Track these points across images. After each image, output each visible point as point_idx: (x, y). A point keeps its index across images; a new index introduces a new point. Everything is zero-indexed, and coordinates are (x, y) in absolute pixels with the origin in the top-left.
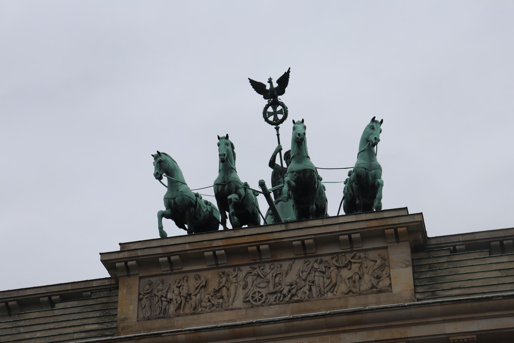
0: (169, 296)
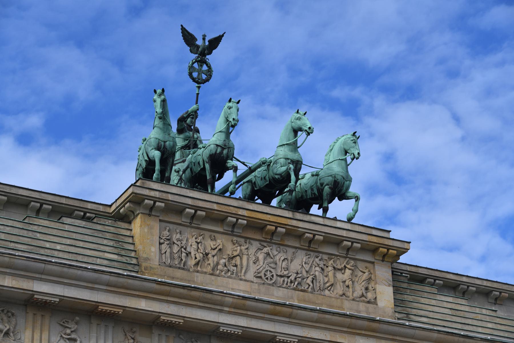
0: (188, 249)
